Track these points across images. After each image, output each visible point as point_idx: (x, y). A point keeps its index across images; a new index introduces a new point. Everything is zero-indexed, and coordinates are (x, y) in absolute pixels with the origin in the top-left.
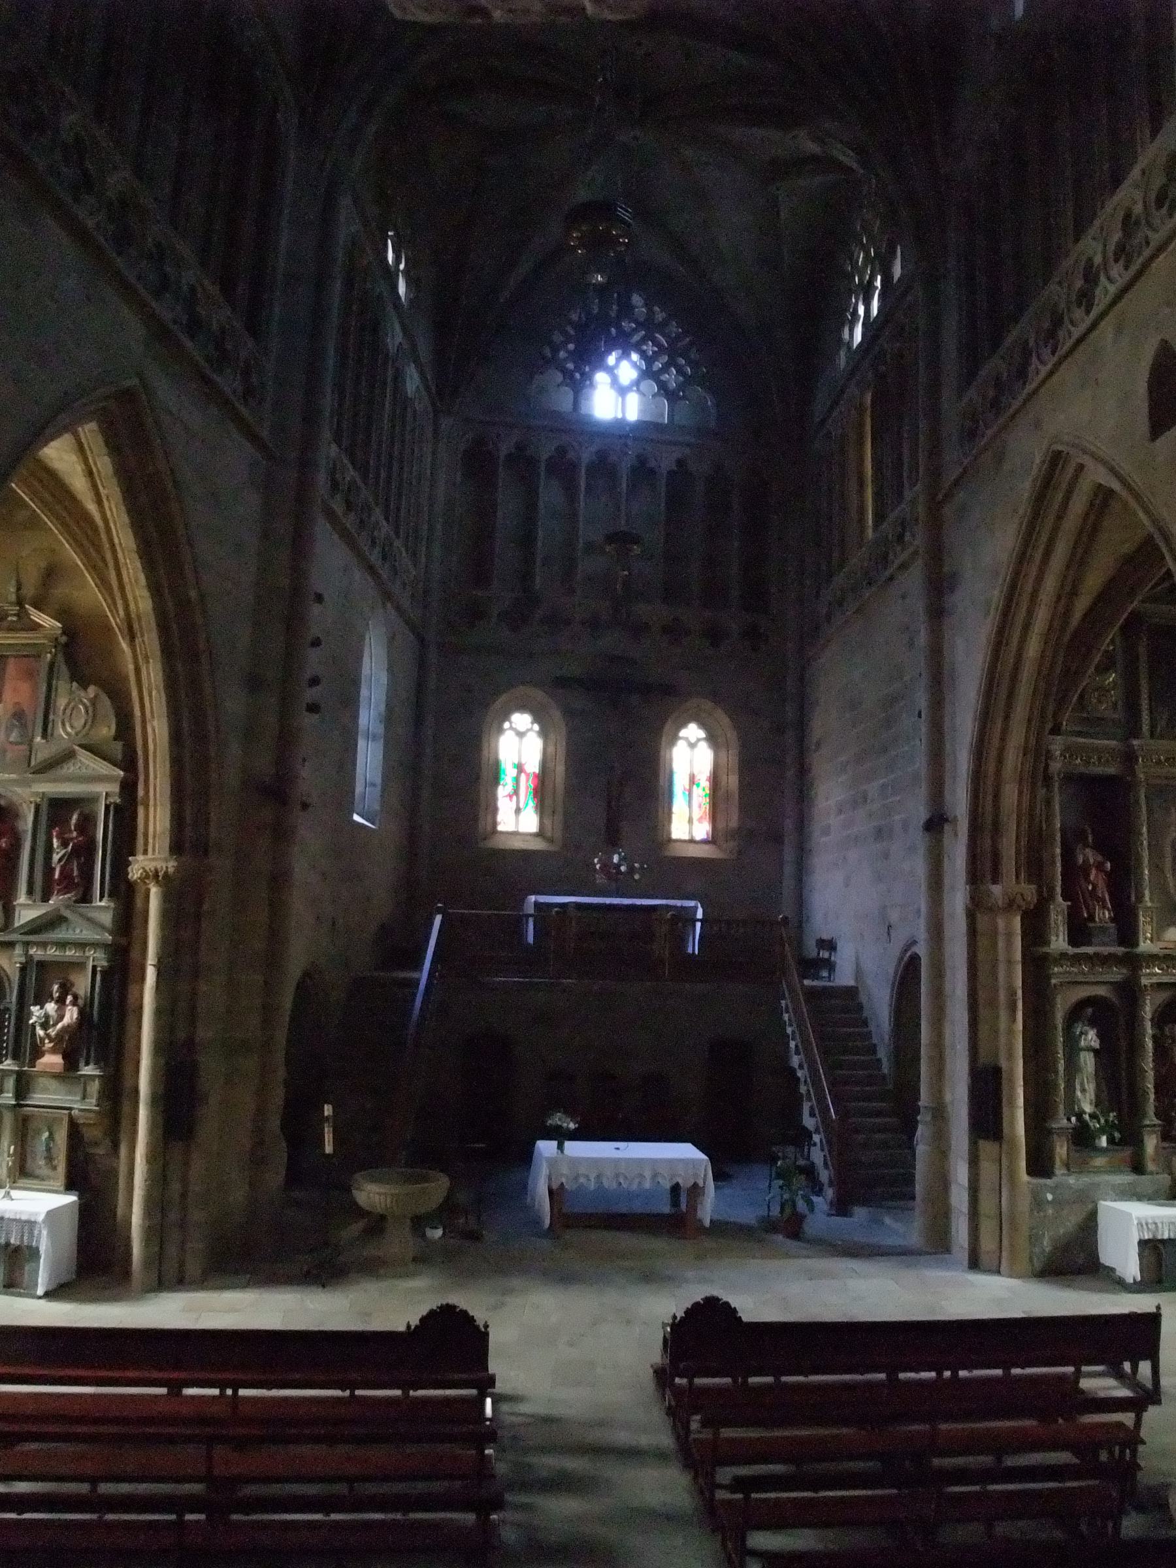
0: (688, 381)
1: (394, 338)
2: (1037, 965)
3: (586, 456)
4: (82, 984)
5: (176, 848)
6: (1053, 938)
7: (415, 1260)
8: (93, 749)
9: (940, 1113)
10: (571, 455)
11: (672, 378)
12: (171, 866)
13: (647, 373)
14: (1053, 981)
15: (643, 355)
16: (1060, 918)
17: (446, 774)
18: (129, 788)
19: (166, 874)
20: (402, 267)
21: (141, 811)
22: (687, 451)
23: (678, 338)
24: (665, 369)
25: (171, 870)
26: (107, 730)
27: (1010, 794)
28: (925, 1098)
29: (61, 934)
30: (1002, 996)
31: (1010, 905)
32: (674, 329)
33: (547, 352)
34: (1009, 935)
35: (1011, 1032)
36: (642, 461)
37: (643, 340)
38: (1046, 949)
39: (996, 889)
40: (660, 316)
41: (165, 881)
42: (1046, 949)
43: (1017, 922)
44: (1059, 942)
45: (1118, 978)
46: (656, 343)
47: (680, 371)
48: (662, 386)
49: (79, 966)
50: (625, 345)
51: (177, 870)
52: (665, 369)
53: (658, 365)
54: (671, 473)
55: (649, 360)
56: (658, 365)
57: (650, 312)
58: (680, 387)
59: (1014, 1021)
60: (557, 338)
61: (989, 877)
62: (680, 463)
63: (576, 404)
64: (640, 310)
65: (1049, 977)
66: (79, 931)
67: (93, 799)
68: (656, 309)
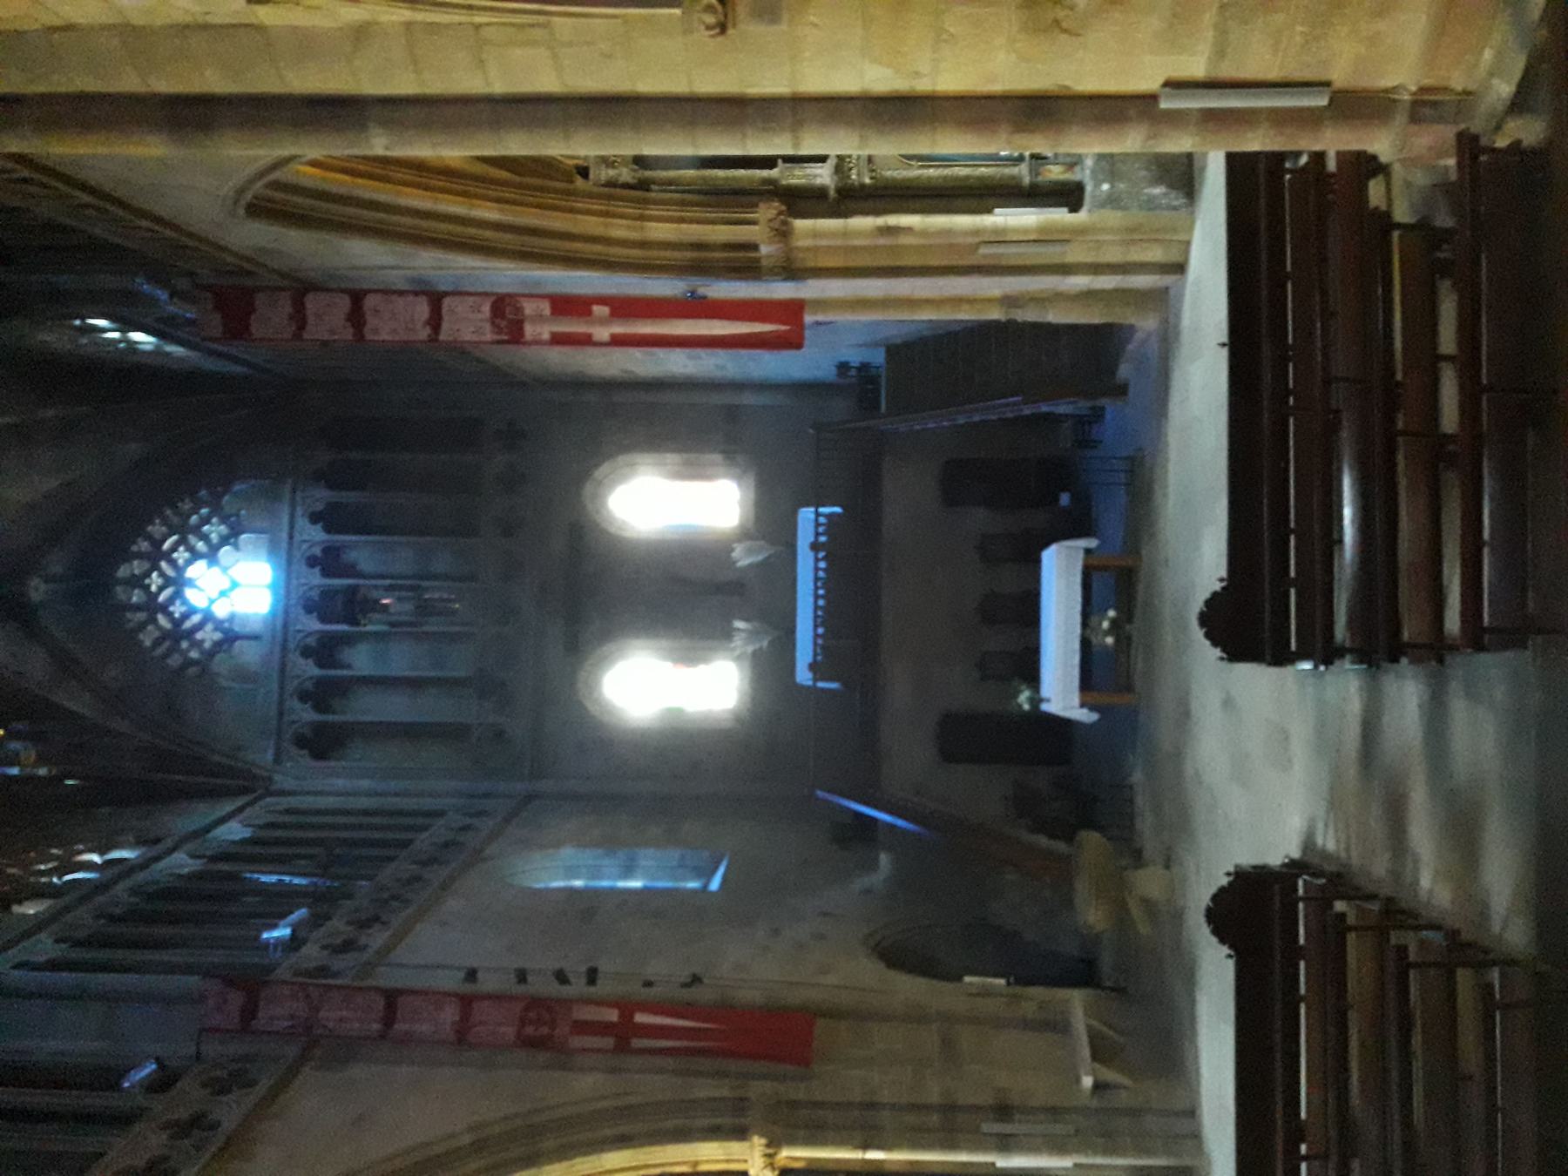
0: (217, 510)
1: (182, 862)
3: (314, 625)
5: (740, 1134)
6: (818, 181)
7: (1167, 867)
9: (1009, 301)
10: (311, 641)
11: (215, 530)
12: (758, 1142)
13: (212, 556)
14: (867, 181)
15: (189, 562)
16: (797, 172)
17: (668, 782)
19: (768, 1146)
20: (96, 858)
21: (704, 1168)
22: (299, 511)
23: (165, 522)
24: (205, 538)
25: (763, 1141)
27: (660, 231)
28: (995, 314)
30: (882, 241)
31: (784, 233)
32: (156, 529)
33: (192, 671)
34: (816, 234)
35: (924, 233)
36: (312, 562)
37: (173, 563)
38: (832, 193)
40: (144, 546)
41: (774, 1143)
42: (832, 193)
43: (800, 224)
46: (174, 549)
47: (207, 521)
48: (224, 541)
50: (178, 583)
51: (762, 1135)
52: (205, 538)
53: (201, 546)
54: (328, 530)
55: (195, 556)
56: (201, 546)
57: (140, 556)
58: (224, 520)
59: (908, 230)
60: (175, 661)
61: (753, 255)
62: (315, 518)
63: (255, 637)
64: (137, 567)
65: (863, 186)
68: (134, 548)
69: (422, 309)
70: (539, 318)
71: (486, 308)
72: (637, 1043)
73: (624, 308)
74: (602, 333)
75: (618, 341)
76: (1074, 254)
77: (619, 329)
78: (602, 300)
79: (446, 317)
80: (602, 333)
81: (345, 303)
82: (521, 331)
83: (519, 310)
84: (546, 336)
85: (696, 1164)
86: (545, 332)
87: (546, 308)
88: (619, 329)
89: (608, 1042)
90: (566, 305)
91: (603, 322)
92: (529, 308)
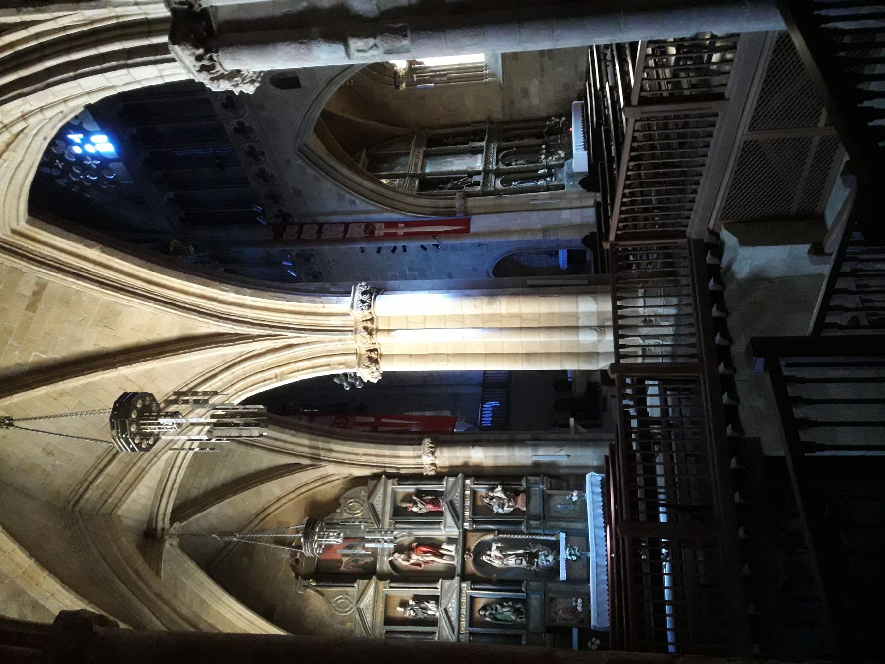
2: (485, 194)
4: (482, 490)
5: (419, 442)
8: (371, 494)
9: (545, 230)
12: (427, 441)
18: (390, 476)
21: (403, 471)
25: (429, 440)
26: (363, 492)
29: (458, 504)
39: (457, 205)
44: (479, 188)
45: (493, 177)
49: (474, 493)
66: (456, 496)
67: (394, 493)
69: (342, 228)
70: (380, 229)
71: (363, 227)
72: (380, 429)
73: (408, 224)
74: (401, 232)
75: (405, 234)
76: (563, 204)
77: (406, 230)
78: (402, 222)
79: (349, 230)
80: (401, 232)
81: (317, 227)
82: (373, 232)
83: (374, 227)
84: (382, 234)
85: (399, 469)
87: (383, 226)
88: (406, 230)
89: (370, 428)
90: (390, 224)
91: (401, 228)
92: (377, 226)
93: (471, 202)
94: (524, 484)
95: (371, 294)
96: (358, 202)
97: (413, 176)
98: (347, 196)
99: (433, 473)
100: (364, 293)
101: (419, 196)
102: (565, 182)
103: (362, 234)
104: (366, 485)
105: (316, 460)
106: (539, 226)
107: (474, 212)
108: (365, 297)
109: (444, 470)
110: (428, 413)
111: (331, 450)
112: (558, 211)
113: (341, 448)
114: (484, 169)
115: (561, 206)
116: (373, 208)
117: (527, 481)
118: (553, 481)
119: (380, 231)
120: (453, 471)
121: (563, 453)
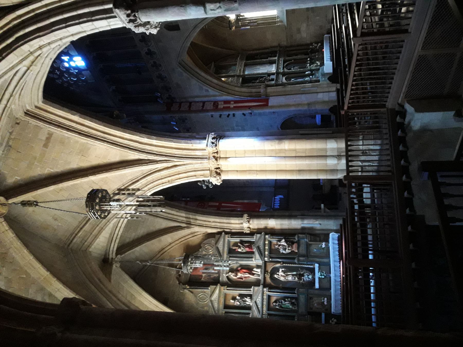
2: (277, 85)
4: (274, 241)
5: (241, 216)
8: (217, 242)
9: (309, 104)
12: (246, 216)
18: (226, 233)
21: (233, 231)
25: (247, 215)
26: (213, 241)
29: (262, 248)
39: (262, 92)
44: (273, 82)
45: (281, 76)
49: (270, 242)
66: (261, 244)
67: (229, 242)
69: (201, 104)
70: (221, 104)
72: (222, 209)
73: (236, 102)
75: (234, 107)
80: (232, 106)
81: (188, 104)
82: (218, 106)
83: (218, 103)
86: (222, 107)
87: (223, 103)
88: (235, 105)
89: (216, 209)
90: (226, 102)
91: (232, 104)
92: (220, 103)
93: (269, 90)
94: (297, 239)
95: (217, 139)
96: (210, 90)
97: (239, 76)
98: (204, 87)
99: (248, 232)
100: (213, 139)
101: (242, 86)
102: (320, 78)
103: (212, 108)
104: (214, 237)
105: (189, 225)
106: (306, 102)
107: (271, 95)
108: (214, 141)
109: (255, 231)
110: (246, 201)
111: (196, 219)
112: (316, 94)
113: (201, 218)
114: (276, 72)
115: (318, 91)
116: (217, 94)
117: (298, 237)
118: (312, 237)
119: (221, 106)
120: (259, 231)
121: (317, 222)
